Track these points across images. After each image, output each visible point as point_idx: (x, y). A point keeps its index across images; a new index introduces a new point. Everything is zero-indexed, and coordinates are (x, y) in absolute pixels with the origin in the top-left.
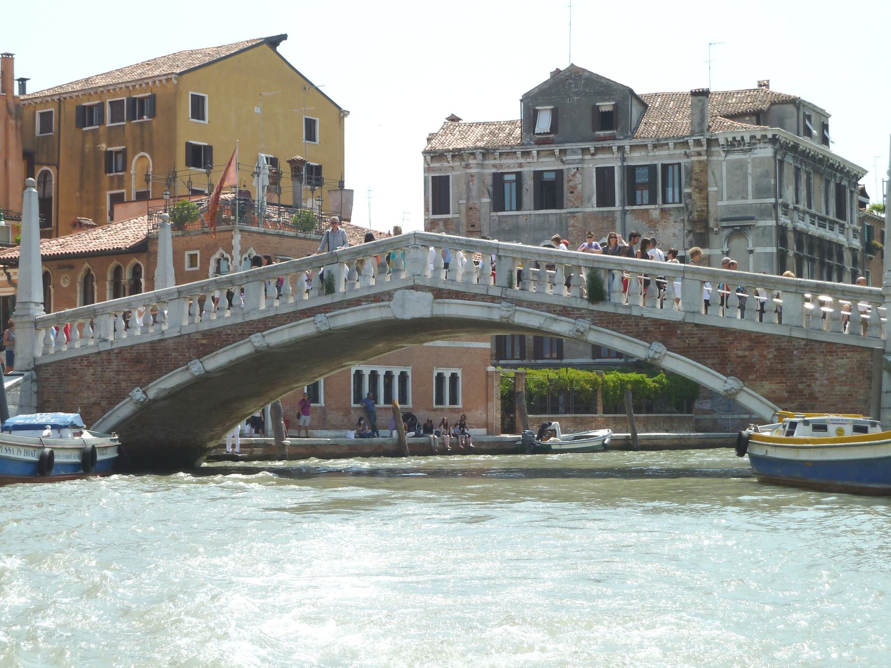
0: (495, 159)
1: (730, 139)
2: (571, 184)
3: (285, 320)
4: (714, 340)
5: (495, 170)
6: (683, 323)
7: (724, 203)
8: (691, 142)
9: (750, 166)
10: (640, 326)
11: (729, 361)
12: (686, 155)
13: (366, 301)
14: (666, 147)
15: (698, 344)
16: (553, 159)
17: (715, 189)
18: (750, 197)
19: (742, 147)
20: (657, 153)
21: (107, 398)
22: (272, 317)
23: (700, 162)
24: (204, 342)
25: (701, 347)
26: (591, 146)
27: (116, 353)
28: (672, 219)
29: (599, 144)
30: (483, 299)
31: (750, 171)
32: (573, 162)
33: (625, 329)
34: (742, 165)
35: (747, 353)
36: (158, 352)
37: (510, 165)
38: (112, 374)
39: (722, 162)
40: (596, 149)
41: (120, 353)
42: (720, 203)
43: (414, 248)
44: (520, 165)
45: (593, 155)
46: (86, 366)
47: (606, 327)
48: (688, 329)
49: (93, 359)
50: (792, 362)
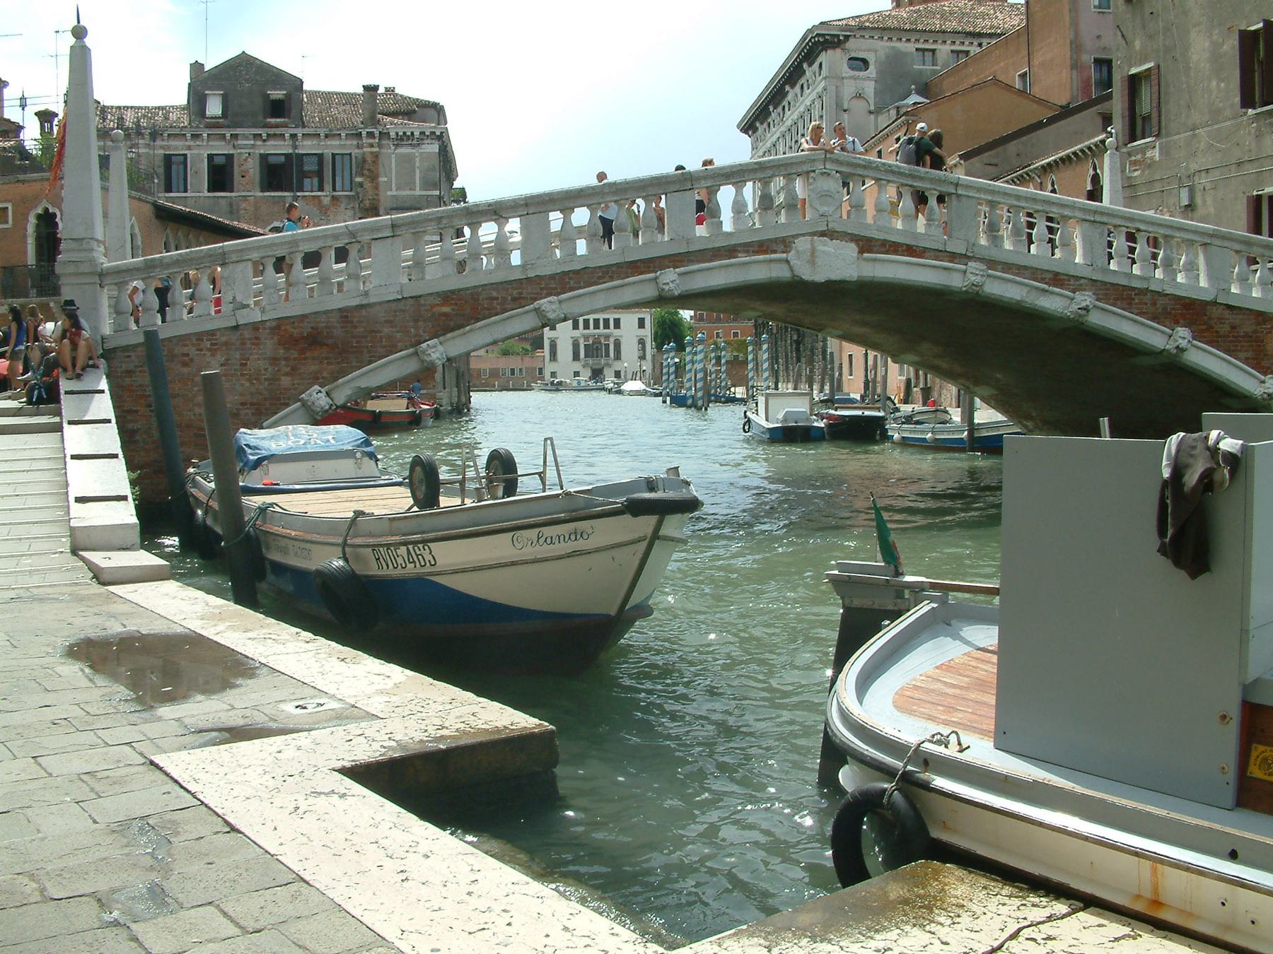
0: (163, 140)
1: (401, 134)
2: (243, 168)
3: (599, 278)
4: (1248, 328)
5: (162, 152)
6: (1214, 303)
7: (394, 193)
8: (364, 133)
9: (417, 159)
10: (1158, 306)
11: (1265, 355)
12: (358, 147)
13: (748, 252)
14: (337, 138)
15: (1230, 332)
16: (223, 143)
17: (386, 179)
18: (418, 188)
19: (410, 142)
20: (329, 143)
21: (252, 404)
22: (576, 272)
23: (372, 153)
24: (446, 309)
25: (1233, 337)
26: (263, 132)
27: (271, 328)
28: (343, 206)
29: (272, 131)
31: (417, 164)
32: (245, 147)
33: (1137, 308)
34: (409, 159)
36: (355, 327)
37: (177, 147)
38: (262, 364)
39: (392, 156)
40: (269, 135)
41: (278, 327)
42: (389, 193)
43: (822, 174)
44: (189, 148)
45: (264, 141)
46: (209, 350)
48: (1217, 312)
49: (223, 339)
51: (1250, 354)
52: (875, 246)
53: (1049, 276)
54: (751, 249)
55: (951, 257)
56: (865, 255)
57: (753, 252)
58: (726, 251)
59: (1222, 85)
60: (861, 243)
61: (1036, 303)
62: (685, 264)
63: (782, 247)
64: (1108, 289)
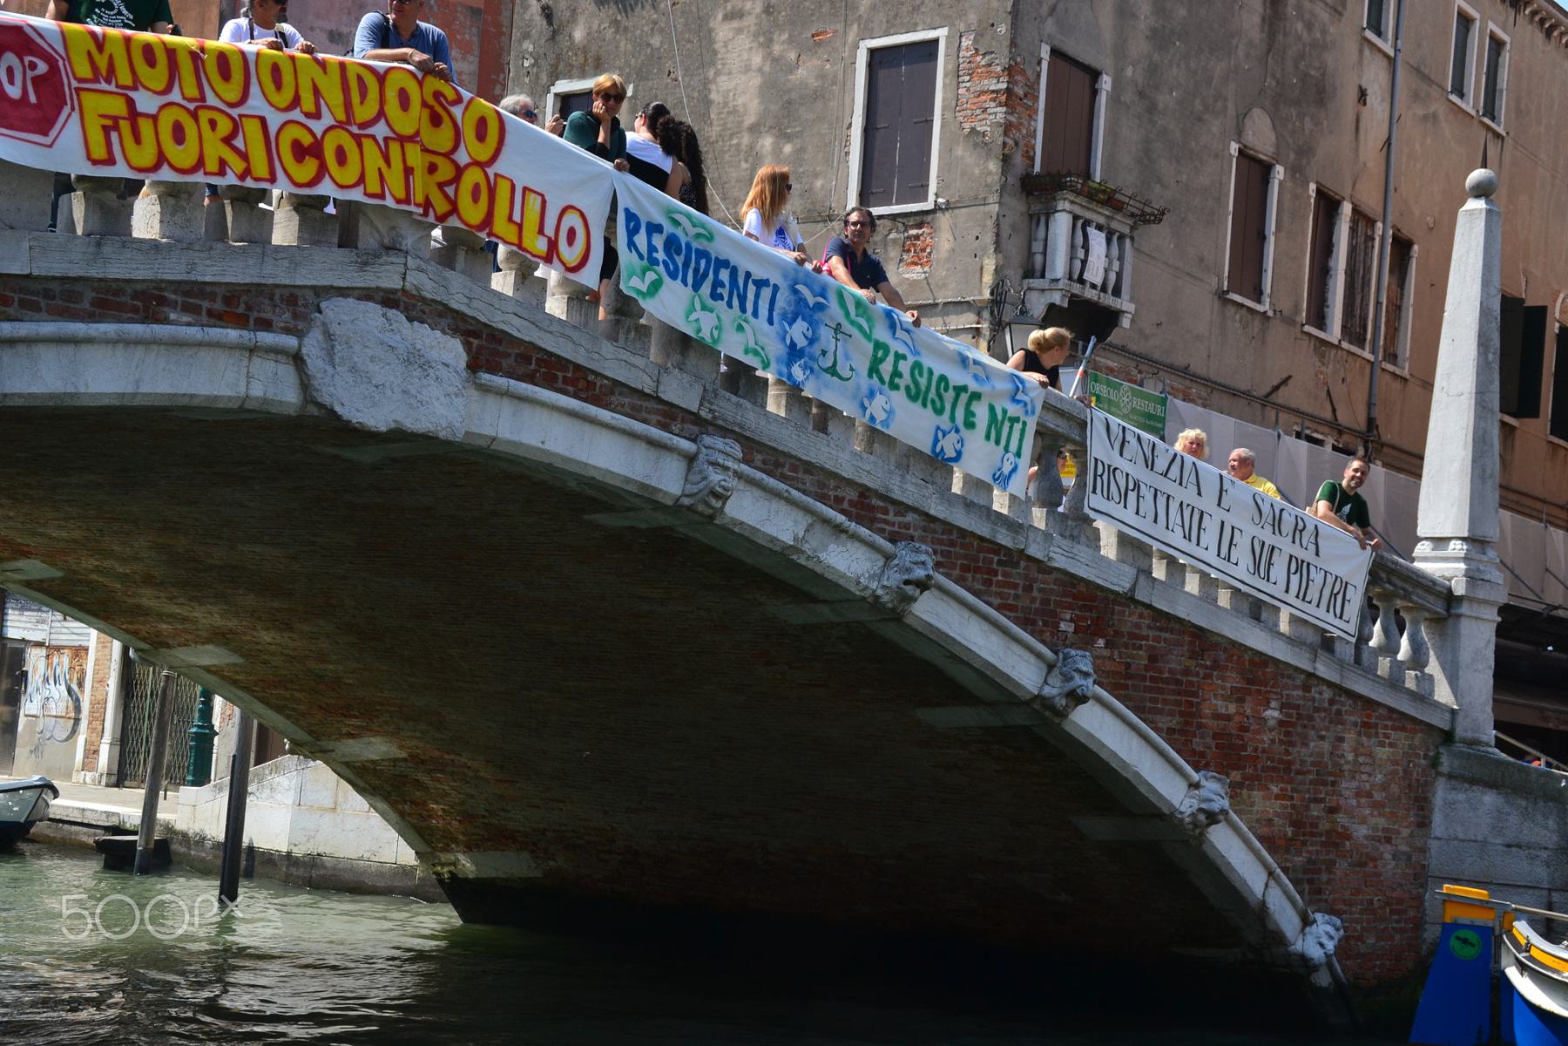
4: (1176, 660)
6: (1129, 599)
10: (1035, 593)
13: (187, 309)
30: (633, 408)
33: (1000, 595)
35: (1232, 709)
47: (960, 581)
50: (1306, 745)
51: (1174, 722)
52: (507, 355)
53: (852, 494)
54: (206, 304)
55: (665, 415)
56: (485, 377)
57: (210, 313)
58: (136, 295)
59: (788, 149)
60: (475, 342)
61: (822, 556)
62: (11, 311)
63: (287, 316)
64: (952, 544)
